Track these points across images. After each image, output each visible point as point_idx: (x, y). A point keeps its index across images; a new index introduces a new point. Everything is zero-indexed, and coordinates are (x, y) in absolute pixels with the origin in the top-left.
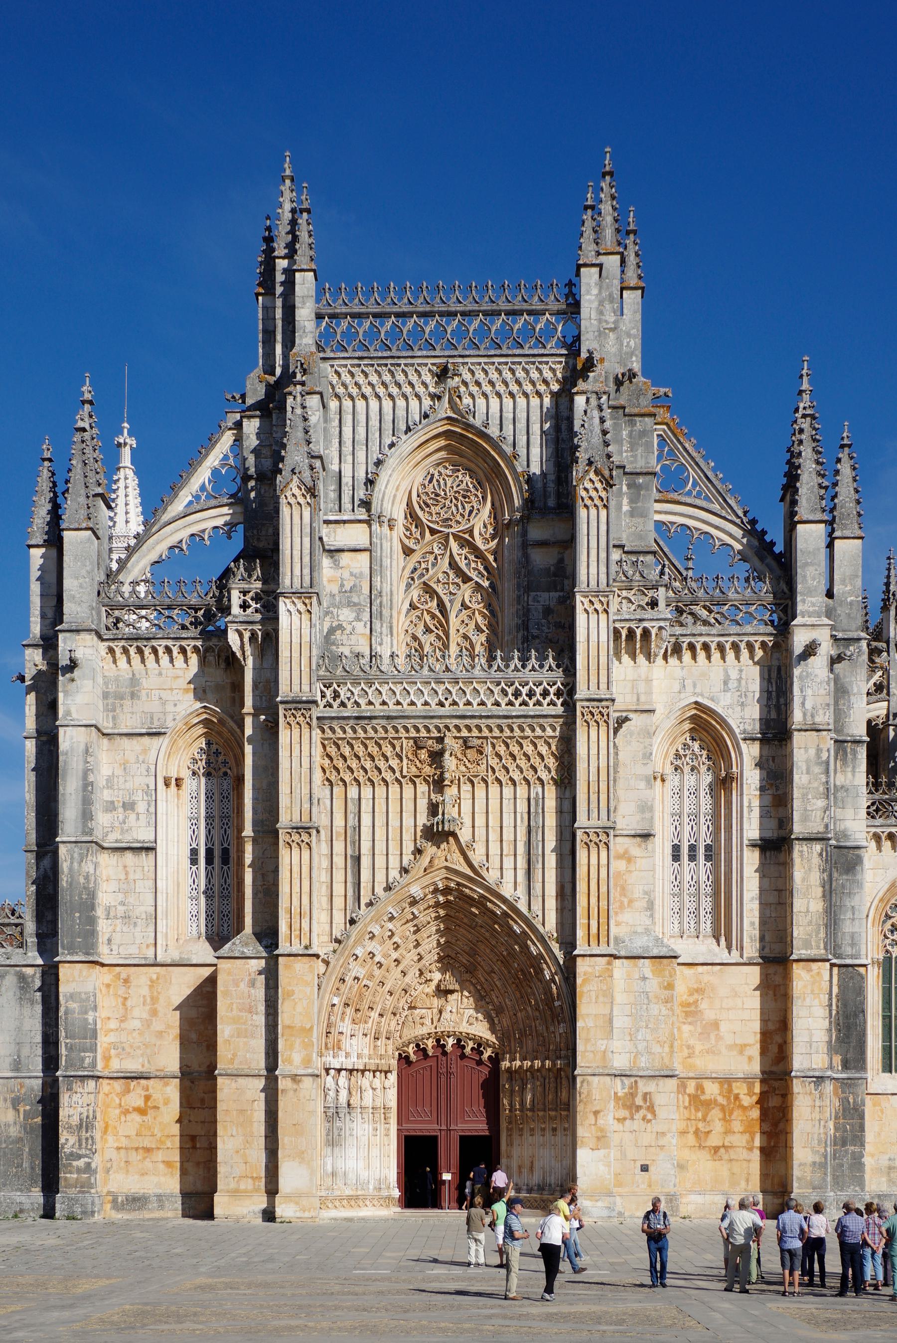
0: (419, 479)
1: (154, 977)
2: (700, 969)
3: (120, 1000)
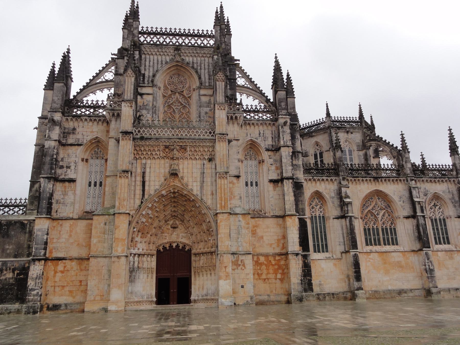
0: (168, 78)
1: (72, 223)
2: (256, 219)
3: (58, 232)
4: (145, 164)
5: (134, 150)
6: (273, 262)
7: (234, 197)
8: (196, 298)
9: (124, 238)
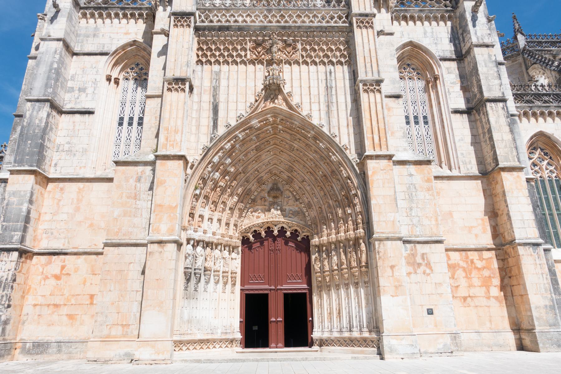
4: (218, 74)
5: (198, 50)
6: (479, 264)
7: (392, 133)
8: (326, 335)
9: (174, 205)
